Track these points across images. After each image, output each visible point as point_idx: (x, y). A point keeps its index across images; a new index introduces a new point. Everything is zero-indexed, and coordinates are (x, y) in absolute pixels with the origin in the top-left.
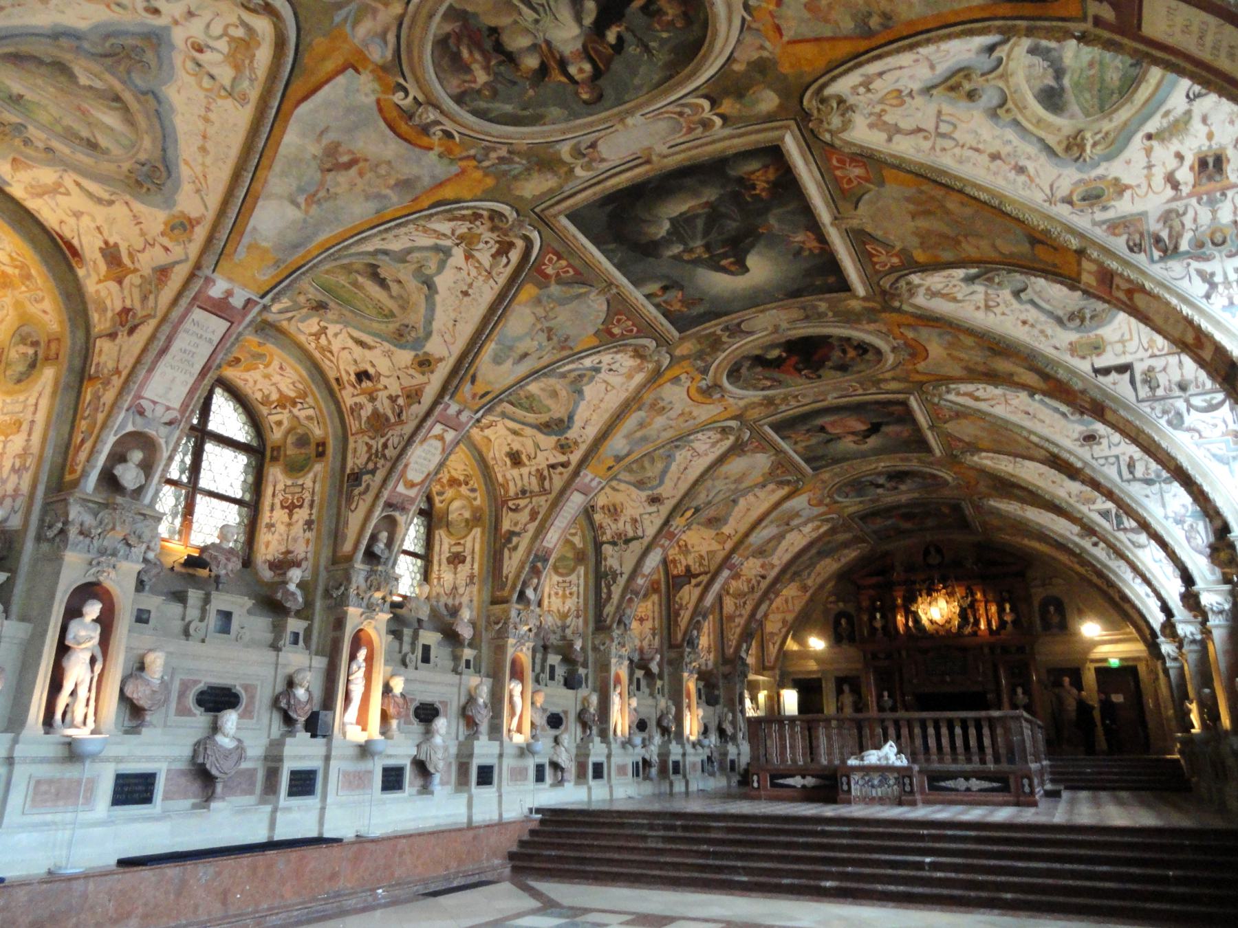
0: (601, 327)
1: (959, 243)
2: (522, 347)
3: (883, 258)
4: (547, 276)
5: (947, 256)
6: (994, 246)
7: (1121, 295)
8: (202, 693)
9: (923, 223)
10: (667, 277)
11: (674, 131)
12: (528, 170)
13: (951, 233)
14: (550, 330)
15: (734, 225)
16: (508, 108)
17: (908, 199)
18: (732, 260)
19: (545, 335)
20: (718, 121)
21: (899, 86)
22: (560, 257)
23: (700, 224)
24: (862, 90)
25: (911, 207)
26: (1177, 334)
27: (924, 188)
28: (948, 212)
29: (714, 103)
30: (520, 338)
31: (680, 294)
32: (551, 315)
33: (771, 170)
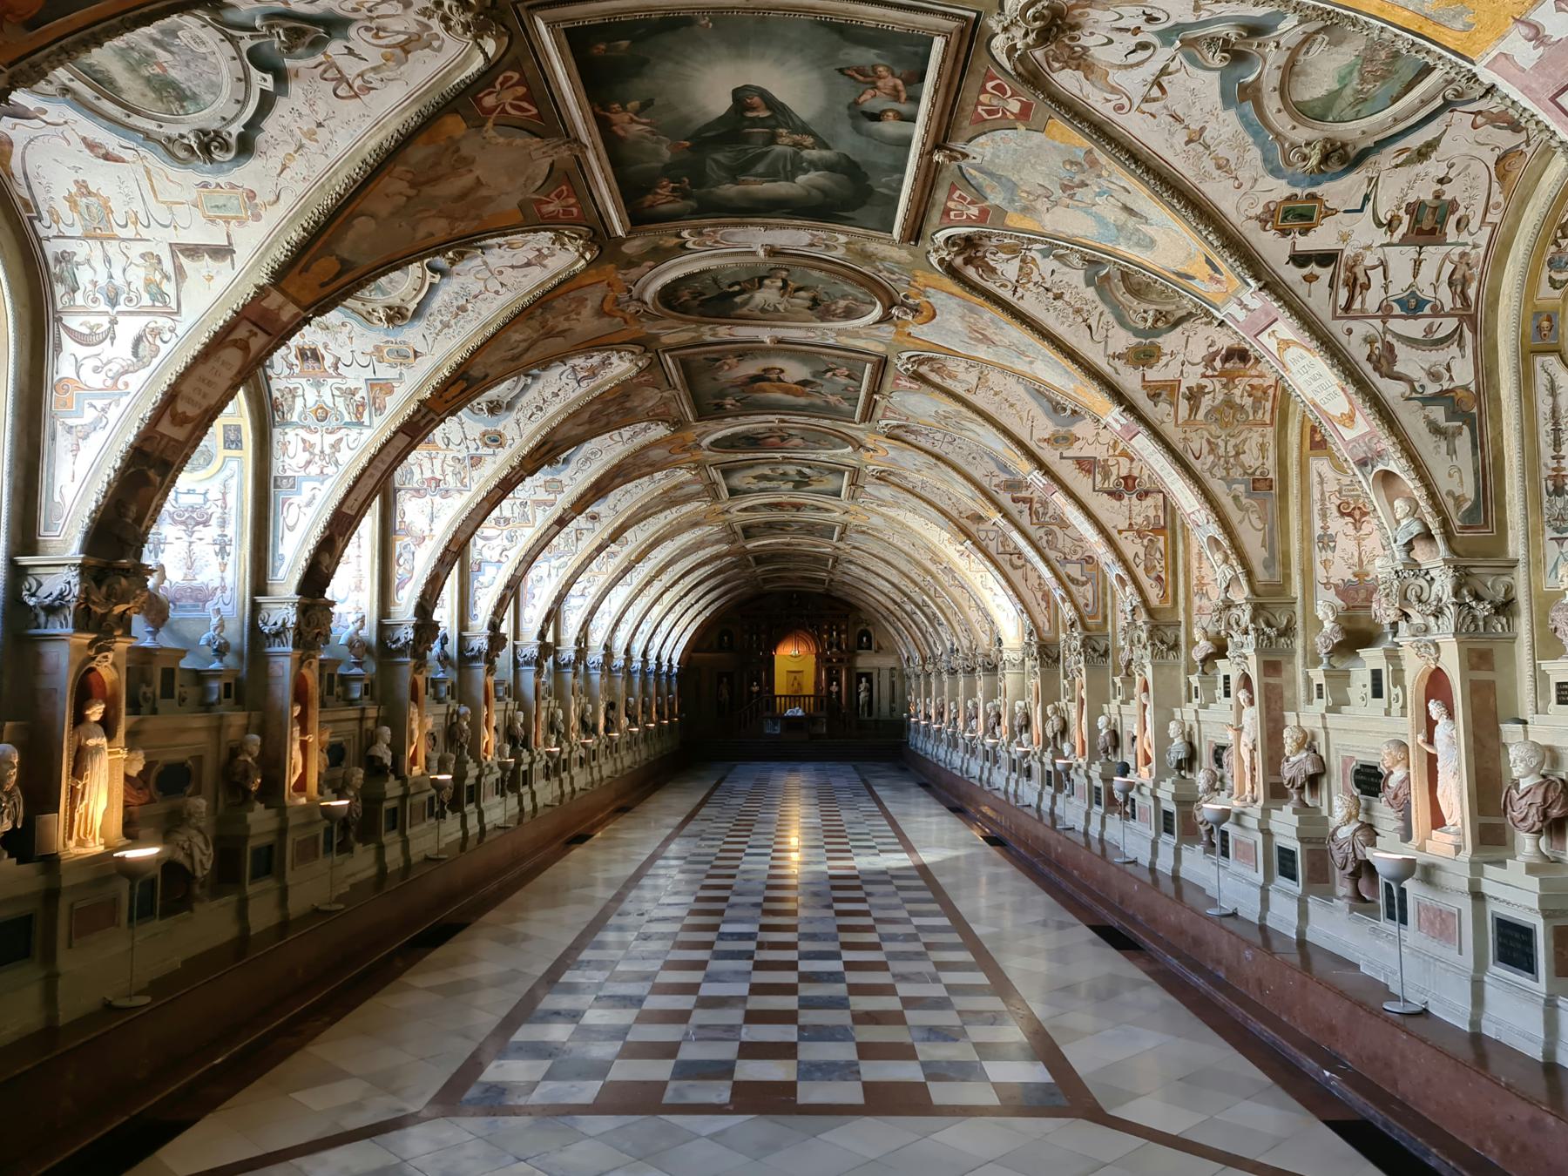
0: (1022, 128)
1: (412, 185)
2: (1113, 215)
3: (508, 97)
4: (984, 213)
5: (418, 153)
6: (373, 216)
7: (241, 333)
8: (1357, 772)
9: (467, 180)
10: (857, 130)
11: (732, 234)
12: (883, 259)
13: (428, 190)
14: (1065, 188)
15: (719, 157)
16: (846, 288)
17: (490, 199)
18: (750, 114)
19: (1080, 192)
20: (685, 234)
21: (511, 252)
22: (947, 212)
23: (760, 168)
24: (545, 251)
25: (484, 192)
26: (186, 389)
27: (475, 223)
28: (441, 214)
29: (683, 246)
30: (1100, 220)
31: (867, 96)
32: (1040, 191)
33: (647, 204)
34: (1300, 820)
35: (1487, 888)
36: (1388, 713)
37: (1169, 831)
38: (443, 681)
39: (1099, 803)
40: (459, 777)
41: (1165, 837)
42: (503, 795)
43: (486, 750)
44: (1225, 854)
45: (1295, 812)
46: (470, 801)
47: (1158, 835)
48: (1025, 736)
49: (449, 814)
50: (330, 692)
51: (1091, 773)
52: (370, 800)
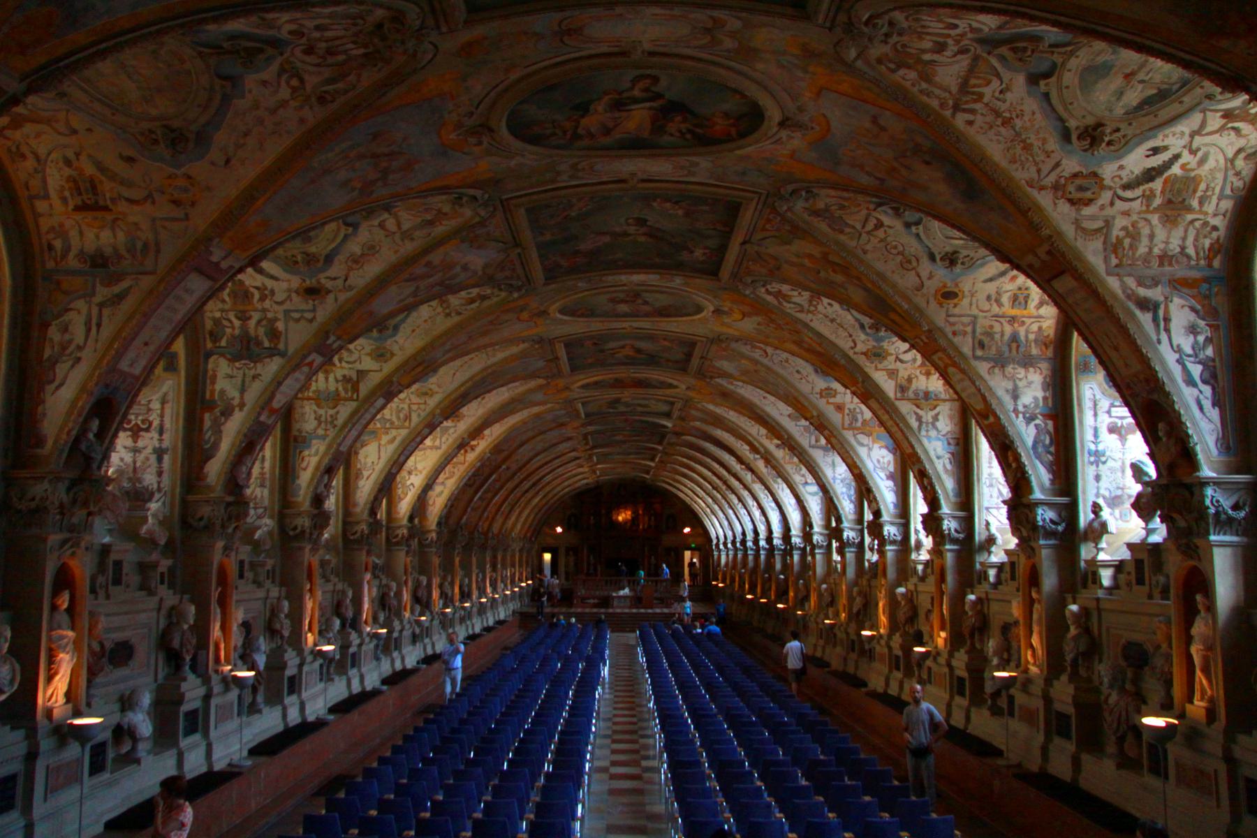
34: (1076, 689)
35: (1237, 752)
36: (1150, 597)
37: (961, 693)
38: (329, 562)
39: (898, 669)
40: (344, 647)
41: (958, 700)
42: (378, 659)
43: (366, 622)
44: (1011, 714)
45: (1070, 681)
46: (353, 666)
47: (952, 697)
48: (831, 611)
49: (337, 678)
50: (241, 576)
51: (892, 644)
52: (275, 664)
